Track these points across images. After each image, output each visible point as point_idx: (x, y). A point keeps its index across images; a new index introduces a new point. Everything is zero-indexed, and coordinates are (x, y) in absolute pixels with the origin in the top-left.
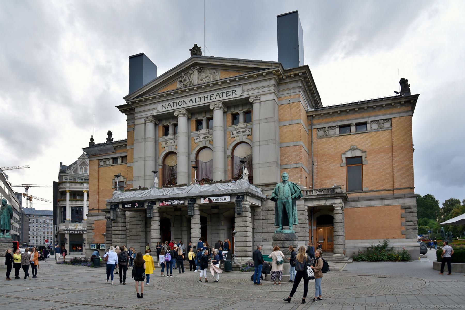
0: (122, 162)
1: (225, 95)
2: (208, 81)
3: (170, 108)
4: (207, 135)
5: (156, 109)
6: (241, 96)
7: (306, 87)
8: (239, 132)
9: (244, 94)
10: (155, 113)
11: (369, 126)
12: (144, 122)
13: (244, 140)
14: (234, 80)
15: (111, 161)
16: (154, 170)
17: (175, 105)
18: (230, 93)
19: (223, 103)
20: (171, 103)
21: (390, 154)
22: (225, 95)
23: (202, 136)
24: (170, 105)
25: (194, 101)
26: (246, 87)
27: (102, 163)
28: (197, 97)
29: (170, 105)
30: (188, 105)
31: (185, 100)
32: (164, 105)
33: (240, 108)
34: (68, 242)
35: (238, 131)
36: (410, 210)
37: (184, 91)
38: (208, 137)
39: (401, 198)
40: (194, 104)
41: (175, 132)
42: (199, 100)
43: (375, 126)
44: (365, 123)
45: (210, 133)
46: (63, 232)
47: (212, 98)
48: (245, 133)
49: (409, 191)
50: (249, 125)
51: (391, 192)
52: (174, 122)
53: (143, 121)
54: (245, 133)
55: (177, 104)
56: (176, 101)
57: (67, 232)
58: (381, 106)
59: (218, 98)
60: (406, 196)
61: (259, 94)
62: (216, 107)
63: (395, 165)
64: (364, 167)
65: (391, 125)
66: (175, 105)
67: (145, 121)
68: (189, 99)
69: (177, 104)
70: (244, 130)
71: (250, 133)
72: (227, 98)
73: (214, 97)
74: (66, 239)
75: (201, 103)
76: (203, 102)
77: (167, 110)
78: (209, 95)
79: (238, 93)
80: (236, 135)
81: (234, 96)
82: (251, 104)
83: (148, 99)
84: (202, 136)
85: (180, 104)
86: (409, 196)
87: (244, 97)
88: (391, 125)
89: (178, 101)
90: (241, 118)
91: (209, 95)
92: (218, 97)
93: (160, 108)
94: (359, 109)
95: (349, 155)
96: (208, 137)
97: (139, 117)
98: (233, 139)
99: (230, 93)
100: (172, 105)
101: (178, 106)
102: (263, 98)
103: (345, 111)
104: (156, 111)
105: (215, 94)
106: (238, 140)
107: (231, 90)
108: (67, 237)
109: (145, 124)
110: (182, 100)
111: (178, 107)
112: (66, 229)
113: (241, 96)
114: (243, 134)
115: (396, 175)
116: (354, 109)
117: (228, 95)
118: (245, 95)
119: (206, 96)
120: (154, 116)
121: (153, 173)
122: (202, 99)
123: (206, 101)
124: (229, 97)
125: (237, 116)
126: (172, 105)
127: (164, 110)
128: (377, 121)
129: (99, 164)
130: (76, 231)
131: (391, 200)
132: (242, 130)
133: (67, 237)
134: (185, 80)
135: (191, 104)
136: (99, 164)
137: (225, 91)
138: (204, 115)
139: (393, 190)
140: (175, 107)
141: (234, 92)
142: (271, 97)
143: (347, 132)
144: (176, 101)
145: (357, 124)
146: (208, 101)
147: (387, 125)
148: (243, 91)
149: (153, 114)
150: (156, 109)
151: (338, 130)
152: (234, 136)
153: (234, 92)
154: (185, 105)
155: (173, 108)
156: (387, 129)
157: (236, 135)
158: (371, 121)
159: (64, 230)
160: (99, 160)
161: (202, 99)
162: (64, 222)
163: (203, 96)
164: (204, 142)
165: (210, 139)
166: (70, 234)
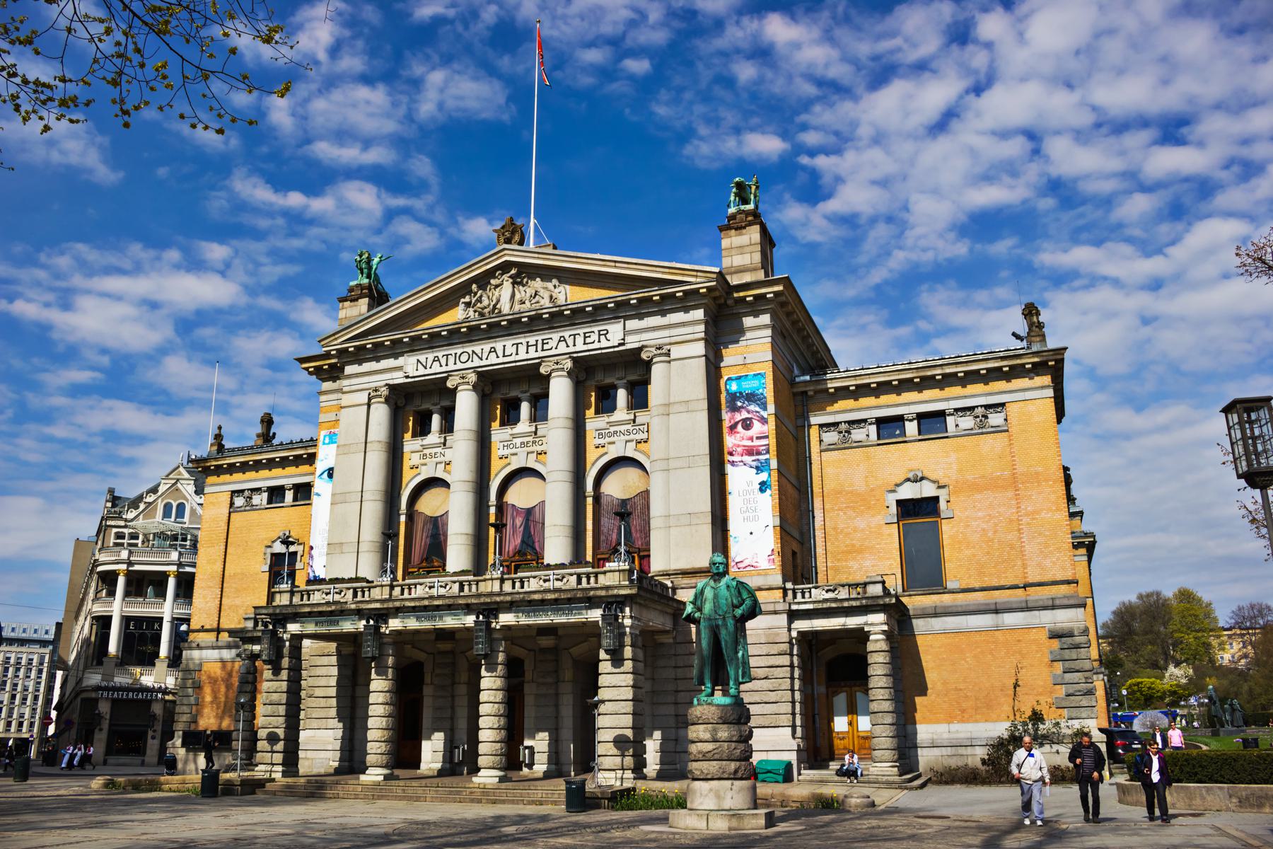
0: (295, 499)
1: (580, 340)
2: (538, 306)
3: (436, 368)
4: (530, 439)
5: (400, 368)
6: (620, 345)
7: (788, 325)
8: (615, 432)
9: (628, 339)
10: (398, 378)
11: (950, 420)
12: (366, 401)
13: (630, 453)
15: (265, 495)
17: (451, 359)
18: (594, 337)
19: (575, 360)
22: (580, 340)
23: (518, 441)
24: (436, 359)
25: (500, 354)
26: (633, 324)
27: (239, 501)
29: (436, 359)
30: (484, 362)
32: (423, 361)
33: (620, 373)
34: (105, 725)
35: (612, 429)
36: (1069, 640)
38: (534, 442)
40: (501, 360)
41: (448, 427)
43: (967, 422)
44: (941, 414)
45: (539, 433)
46: (93, 695)
47: (546, 347)
48: (632, 437)
49: (1064, 589)
50: (642, 417)
52: (446, 403)
53: (363, 397)
54: (632, 437)
55: (457, 357)
56: (453, 352)
57: (105, 694)
59: (562, 348)
60: (1057, 602)
61: (667, 341)
62: (558, 370)
66: (451, 359)
67: (370, 399)
68: (487, 347)
69: (457, 357)
70: (629, 427)
71: (644, 436)
72: (586, 347)
73: (552, 344)
74: (100, 716)
75: (518, 358)
76: (522, 355)
77: (428, 371)
79: (613, 336)
80: (608, 440)
81: (604, 343)
82: (648, 365)
85: (464, 358)
86: (1066, 602)
87: (628, 346)
89: (459, 351)
90: (622, 395)
91: (540, 338)
93: (411, 367)
96: (534, 442)
97: (354, 388)
98: (601, 450)
99: (594, 337)
100: (443, 361)
101: (459, 364)
102: (676, 352)
104: (401, 374)
105: (555, 337)
106: (613, 452)
107: (596, 329)
108: (104, 708)
109: (369, 405)
111: (460, 366)
112: (104, 684)
113: (620, 345)
114: (627, 438)
117: (588, 340)
118: (632, 343)
120: (393, 388)
122: (522, 349)
123: (532, 354)
124: (590, 347)
125: (612, 392)
126: (443, 362)
127: (422, 371)
128: (972, 409)
129: (232, 504)
130: (133, 690)
133: (104, 708)
134: (480, 300)
135: (493, 359)
136: (232, 504)
137: (581, 331)
138: (525, 387)
140: (451, 367)
141: (604, 334)
143: (896, 436)
145: (921, 417)
146: (537, 355)
147: (995, 419)
148: (626, 333)
149: (391, 382)
152: (602, 441)
153: (604, 334)
154: (477, 362)
155: (444, 369)
156: (997, 430)
157: (608, 440)
158: (957, 410)
159: (98, 688)
160: (233, 492)
161: (522, 349)
162: (100, 663)
163: (524, 341)
164: (522, 456)
165: (539, 449)
166: (115, 702)
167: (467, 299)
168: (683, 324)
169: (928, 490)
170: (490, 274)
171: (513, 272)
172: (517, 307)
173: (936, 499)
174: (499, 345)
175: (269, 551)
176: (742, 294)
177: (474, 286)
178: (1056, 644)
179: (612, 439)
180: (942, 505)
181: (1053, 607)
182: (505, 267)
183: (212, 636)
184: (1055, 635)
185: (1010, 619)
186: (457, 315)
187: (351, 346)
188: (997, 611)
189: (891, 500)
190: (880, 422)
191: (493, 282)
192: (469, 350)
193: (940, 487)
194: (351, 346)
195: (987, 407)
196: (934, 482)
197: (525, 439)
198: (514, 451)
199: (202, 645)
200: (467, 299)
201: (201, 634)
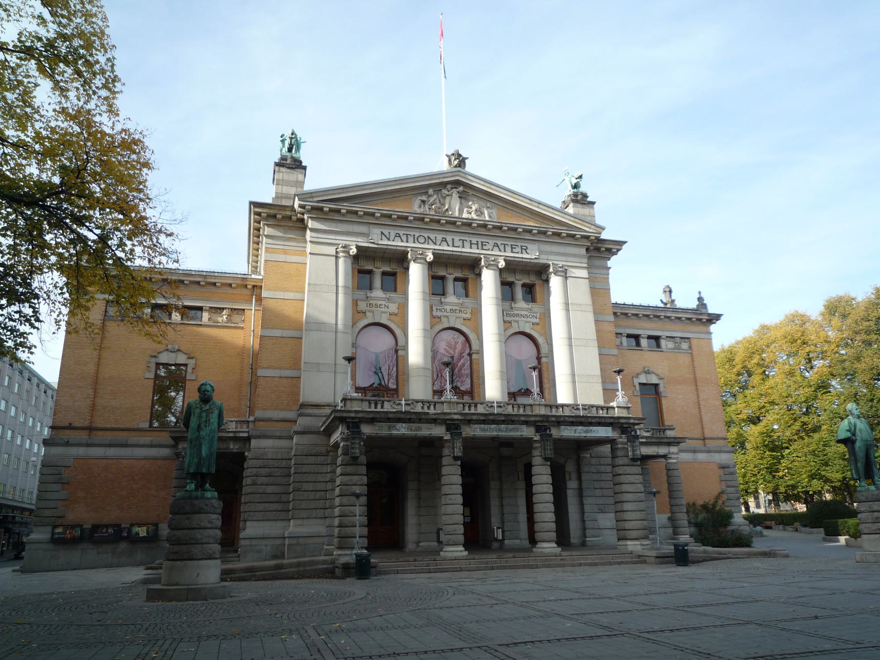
1: (508, 249)
8: (518, 315)
11: (663, 343)
12: (334, 253)
13: (528, 331)
14: (545, 233)
16: (349, 355)
17: (411, 239)
18: (518, 249)
20: (401, 233)
21: (694, 388)
23: (448, 308)
25: (450, 243)
28: (457, 238)
30: (437, 247)
31: (432, 236)
35: (516, 312)
37: (438, 221)
39: (716, 452)
40: (450, 249)
42: (460, 243)
47: (484, 247)
48: (529, 319)
51: (701, 442)
53: (332, 250)
56: (412, 233)
58: (679, 318)
63: (702, 403)
64: (664, 401)
65: (690, 347)
66: (411, 239)
67: (337, 252)
68: (440, 237)
72: (512, 255)
73: (489, 246)
75: (463, 250)
76: (467, 250)
78: (480, 240)
79: (532, 254)
83: (338, 211)
84: (448, 308)
85: (422, 240)
88: (690, 347)
89: (417, 234)
91: (480, 240)
92: (496, 248)
94: (655, 316)
95: (643, 379)
103: (637, 315)
104: (365, 239)
105: (492, 242)
106: (515, 328)
110: (426, 235)
115: (705, 419)
116: (647, 316)
117: (514, 250)
119: (474, 241)
121: (347, 362)
122: (467, 244)
124: (516, 255)
127: (386, 242)
131: (706, 455)
132: (523, 313)
136: (106, 311)
137: (510, 243)
138: (450, 270)
139: (704, 439)
142: (584, 273)
144: (412, 233)
145: (650, 337)
147: (685, 346)
150: (366, 235)
151: (624, 339)
153: (524, 249)
161: (467, 244)
167: (424, 198)
168: (575, 256)
169: (654, 380)
170: (444, 185)
171: (461, 189)
172: (465, 215)
173: (656, 386)
174: (449, 238)
175: (154, 360)
176: (599, 245)
177: (431, 191)
178: (721, 471)
179: (515, 318)
180: (661, 388)
181: (720, 452)
182: (457, 183)
183: (83, 436)
184: (723, 467)
185: (701, 456)
186: (415, 207)
187: (327, 207)
188: (694, 452)
189: (636, 381)
190: (629, 336)
191: (445, 191)
192: (426, 235)
193: (661, 379)
194: (327, 207)
195: (682, 338)
196: (658, 375)
197: (454, 308)
198: (445, 314)
199: (71, 441)
200: (424, 198)
201: (67, 432)
